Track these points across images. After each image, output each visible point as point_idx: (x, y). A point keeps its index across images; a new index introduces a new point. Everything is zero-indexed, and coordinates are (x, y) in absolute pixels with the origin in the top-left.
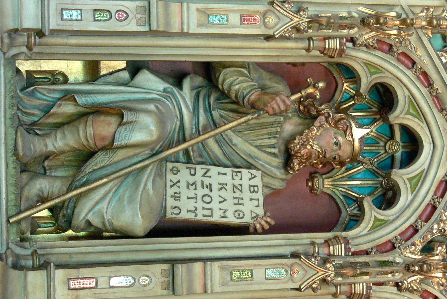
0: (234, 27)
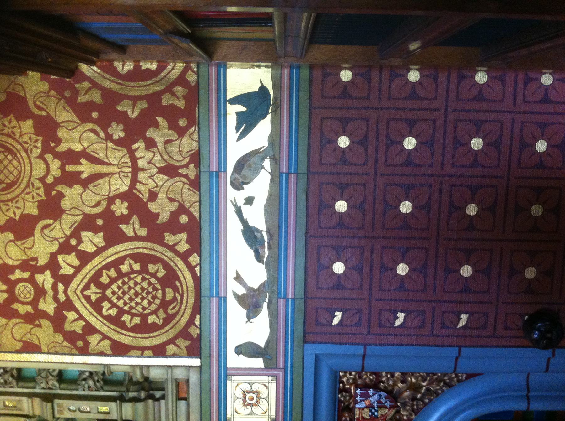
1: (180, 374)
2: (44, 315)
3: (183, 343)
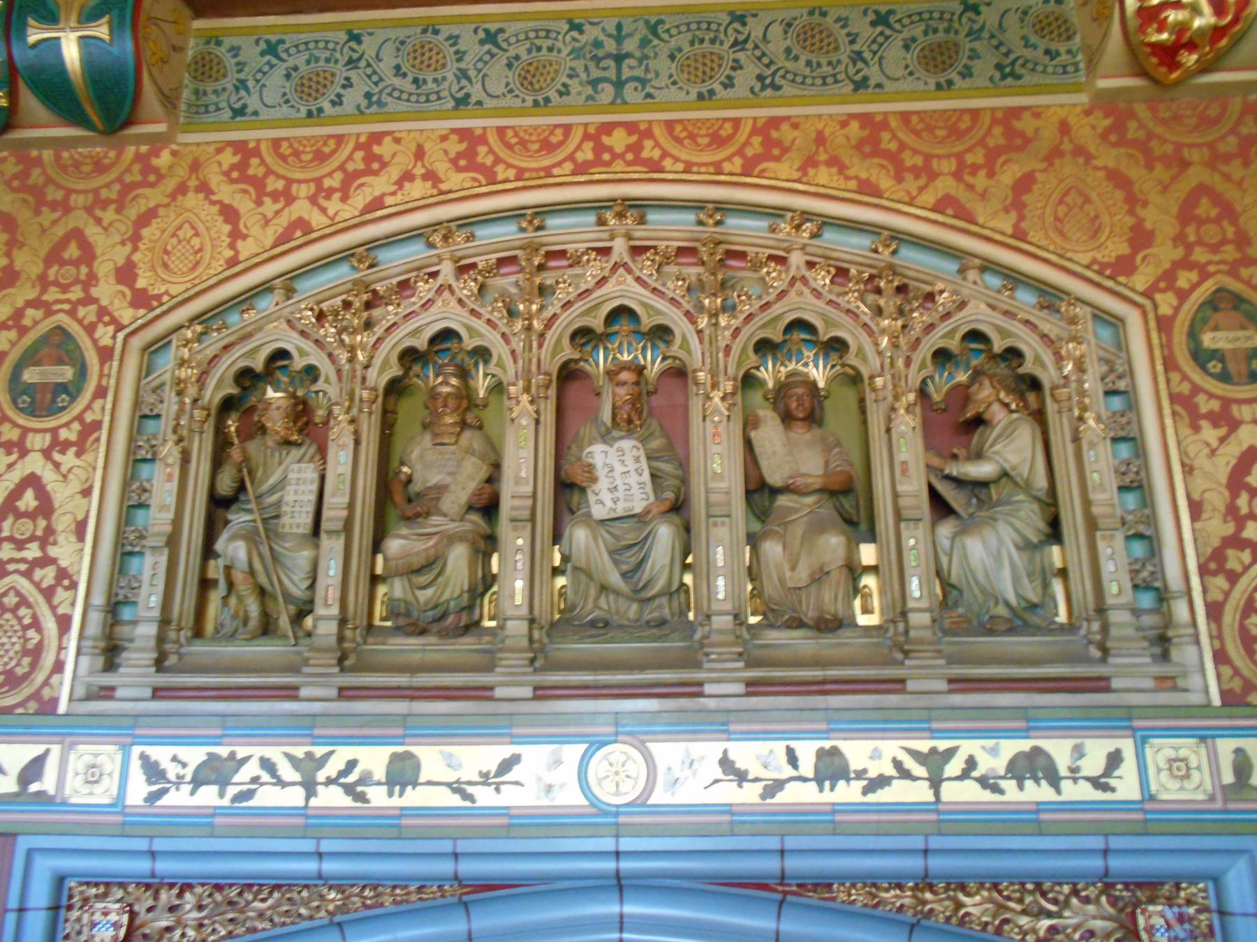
1: (1195, 681)
2: (1240, 526)
3: (1236, 685)
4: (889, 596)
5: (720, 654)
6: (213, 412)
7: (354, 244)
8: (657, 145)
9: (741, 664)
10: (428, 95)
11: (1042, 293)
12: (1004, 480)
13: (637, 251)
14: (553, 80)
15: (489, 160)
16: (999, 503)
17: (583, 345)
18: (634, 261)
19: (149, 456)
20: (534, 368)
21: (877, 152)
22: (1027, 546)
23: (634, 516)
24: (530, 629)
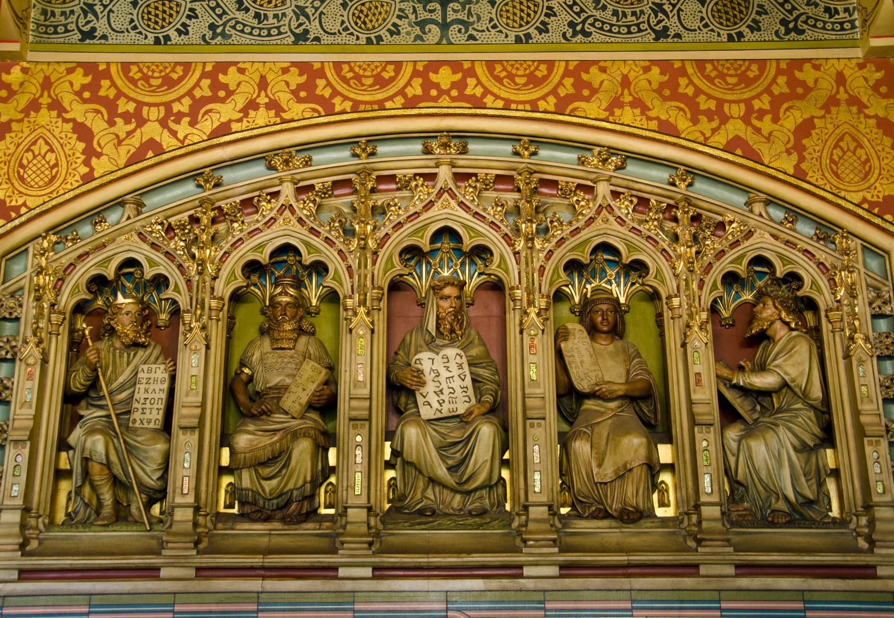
0: (33, 384)
4: (684, 492)
5: (537, 540)
6: (68, 316)
7: (202, 165)
8: (479, 83)
9: (556, 550)
10: (269, 30)
11: (819, 226)
12: (784, 390)
13: (459, 177)
14: (384, 20)
15: (327, 93)
16: (779, 411)
17: (408, 260)
18: (458, 187)
19: (9, 356)
20: (369, 283)
21: (676, 96)
22: (803, 449)
23: (458, 416)
24: (368, 516)
